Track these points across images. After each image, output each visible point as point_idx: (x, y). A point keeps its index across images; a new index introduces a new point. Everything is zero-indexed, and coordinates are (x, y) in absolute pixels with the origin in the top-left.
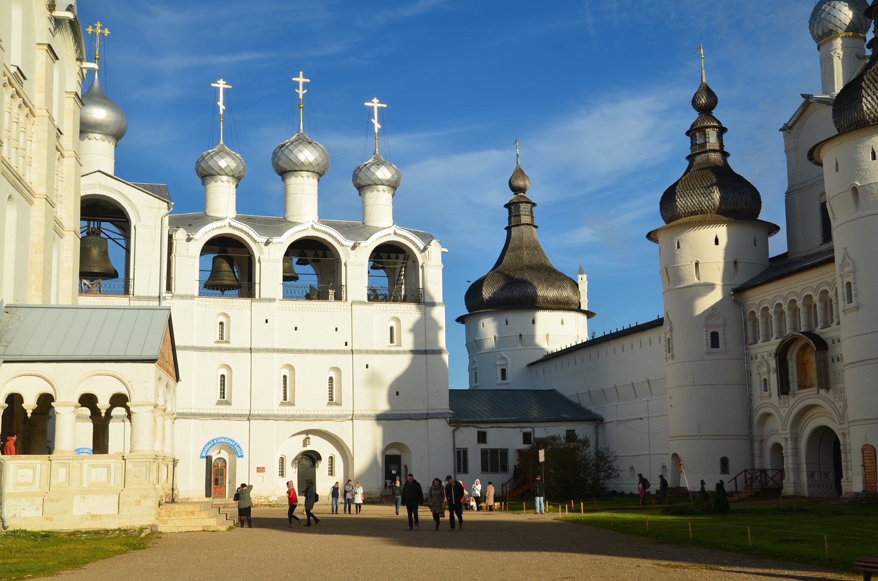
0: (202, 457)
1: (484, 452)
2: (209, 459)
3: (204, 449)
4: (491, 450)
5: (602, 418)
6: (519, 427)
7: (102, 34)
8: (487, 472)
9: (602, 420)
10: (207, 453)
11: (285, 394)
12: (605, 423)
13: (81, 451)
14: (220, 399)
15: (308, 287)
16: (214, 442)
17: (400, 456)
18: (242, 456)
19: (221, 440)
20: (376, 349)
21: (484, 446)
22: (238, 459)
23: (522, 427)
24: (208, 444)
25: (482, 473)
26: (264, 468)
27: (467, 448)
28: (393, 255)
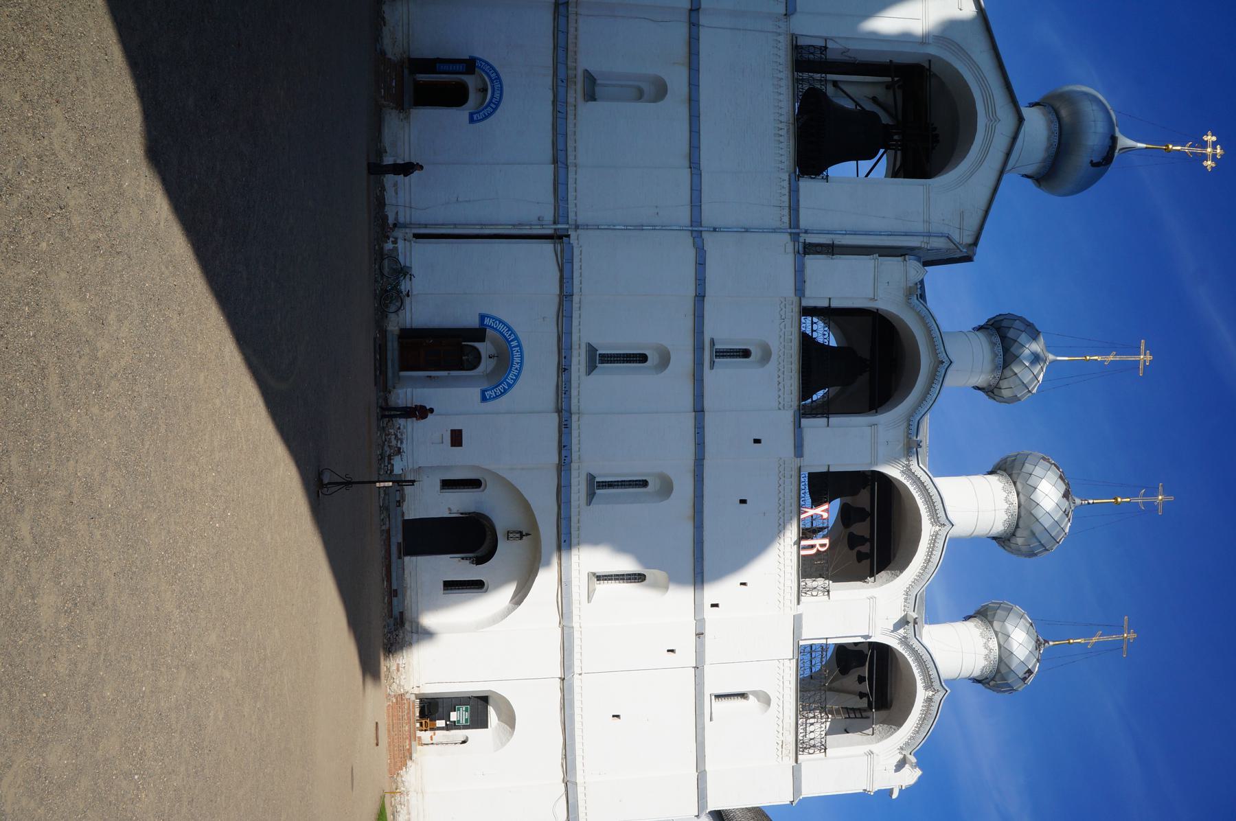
0: (482, 317)
2: (478, 334)
7: (1205, 157)
10: (490, 326)
11: (610, 485)
13: (497, 85)
14: (598, 353)
15: (823, 523)
16: (512, 341)
17: (486, 726)
18: (484, 399)
20: (707, 669)
22: (475, 392)
24: (509, 329)
26: (460, 444)
28: (865, 687)
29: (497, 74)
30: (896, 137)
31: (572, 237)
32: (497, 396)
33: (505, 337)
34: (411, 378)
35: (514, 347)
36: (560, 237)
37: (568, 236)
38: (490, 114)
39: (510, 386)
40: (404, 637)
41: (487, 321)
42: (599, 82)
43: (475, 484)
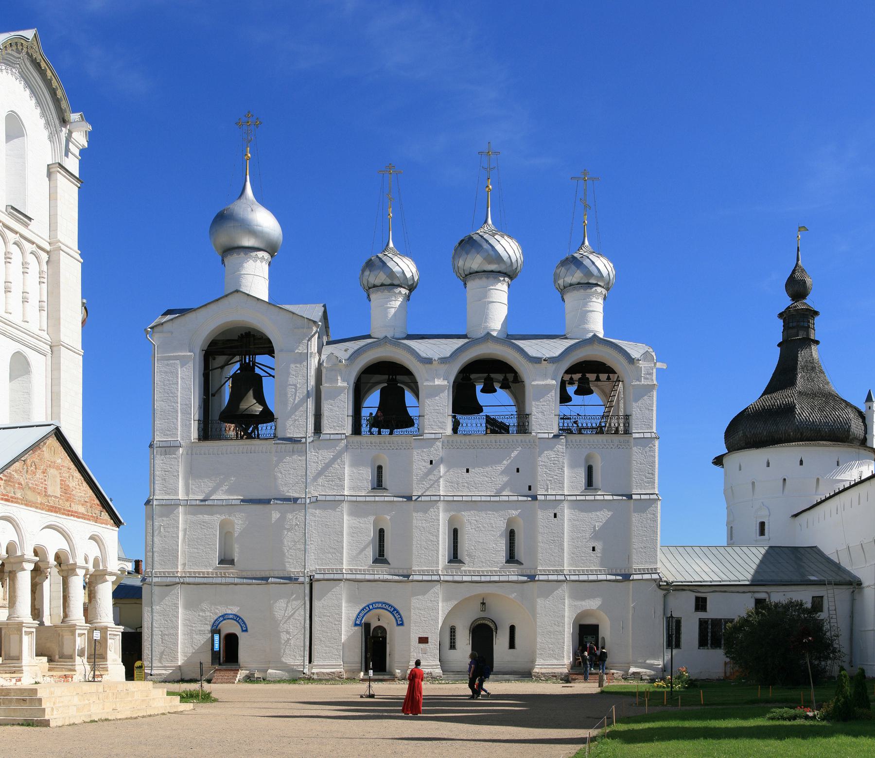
0: (356, 625)
1: (703, 623)
3: (359, 615)
4: (712, 620)
5: (860, 581)
6: (750, 592)
8: (706, 648)
9: (859, 584)
12: (864, 588)
16: (369, 608)
19: (377, 605)
21: (702, 615)
23: (754, 592)
24: (363, 609)
25: (699, 649)
26: (427, 638)
27: (681, 618)
28: (603, 377)
29: (221, 617)
30: (247, 361)
31: (311, 574)
32: (401, 617)
33: (367, 612)
34: (389, 665)
35: (373, 606)
36: (311, 580)
37: (311, 576)
38: (243, 621)
39: (395, 609)
40: (536, 672)
41: (358, 622)
42: (223, 558)
43: (453, 631)
